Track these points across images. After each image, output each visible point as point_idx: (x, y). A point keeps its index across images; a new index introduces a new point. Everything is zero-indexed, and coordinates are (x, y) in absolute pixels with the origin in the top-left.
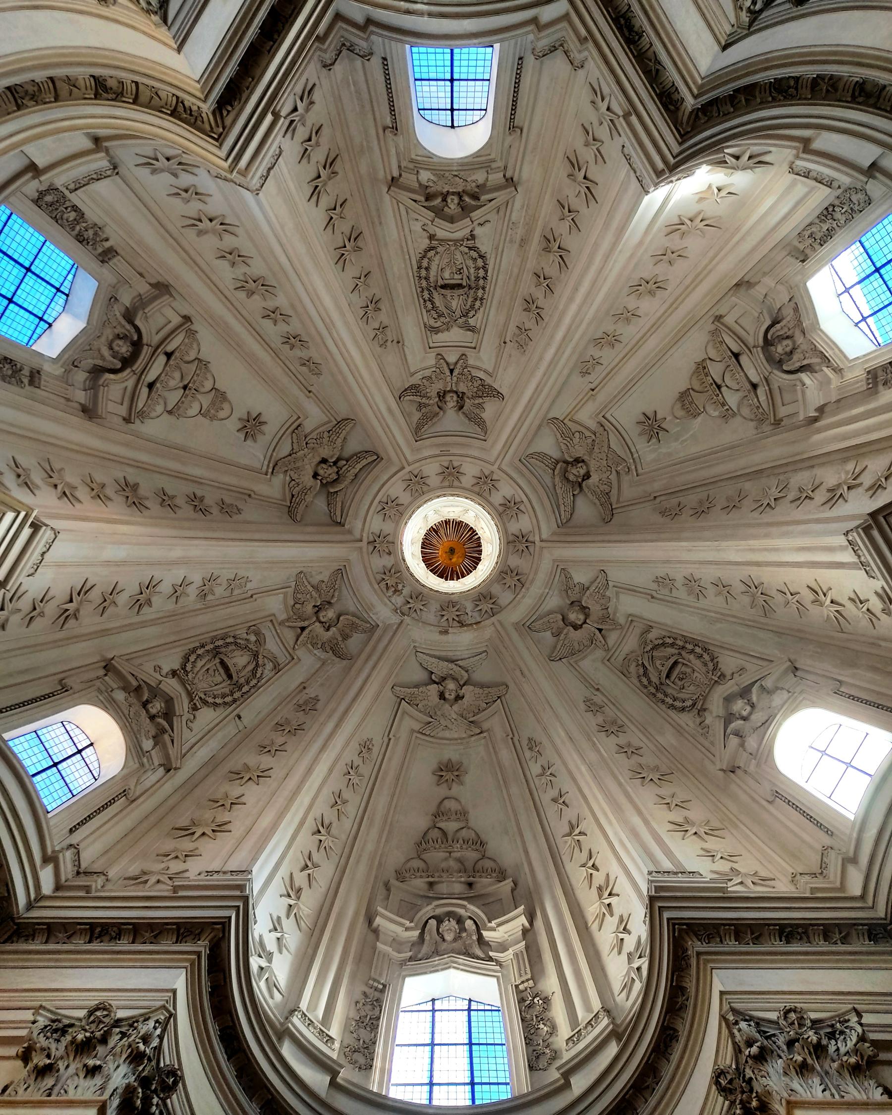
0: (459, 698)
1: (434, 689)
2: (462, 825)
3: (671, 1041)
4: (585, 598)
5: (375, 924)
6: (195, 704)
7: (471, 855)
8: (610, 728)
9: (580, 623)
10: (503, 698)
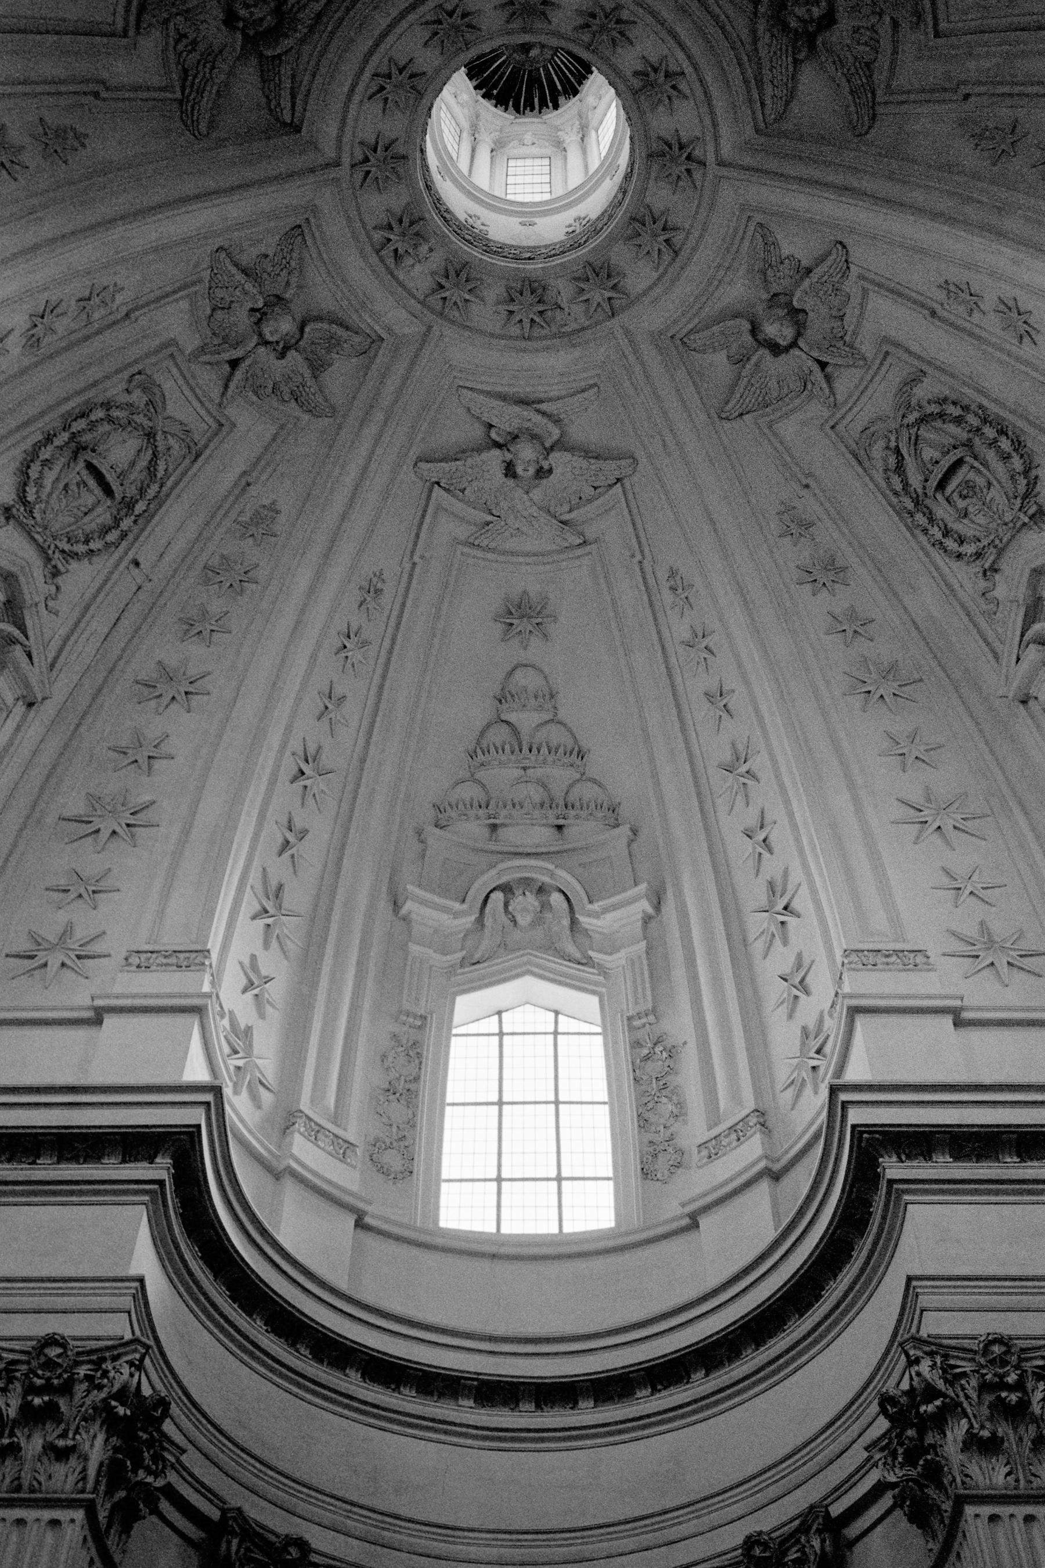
0: (542, 473)
1: (495, 458)
2: (547, 716)
4: (798, 294)
5: (403, 911)
6: (55, 567)
7: (560, 776)
8: (825, 573)
9: (783, 343)
10: (625, 481)
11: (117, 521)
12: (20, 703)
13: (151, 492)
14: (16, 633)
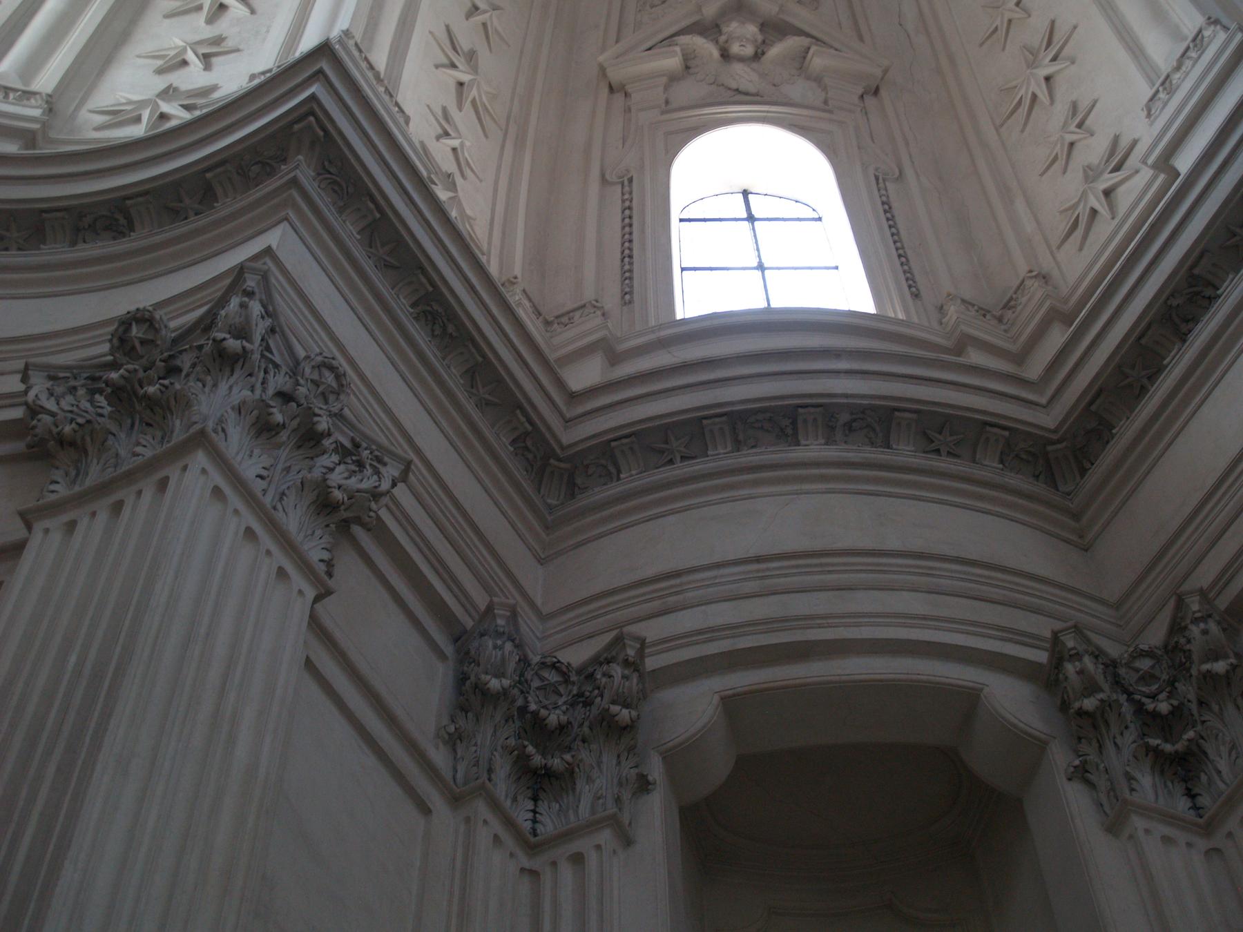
3: (107, 229)
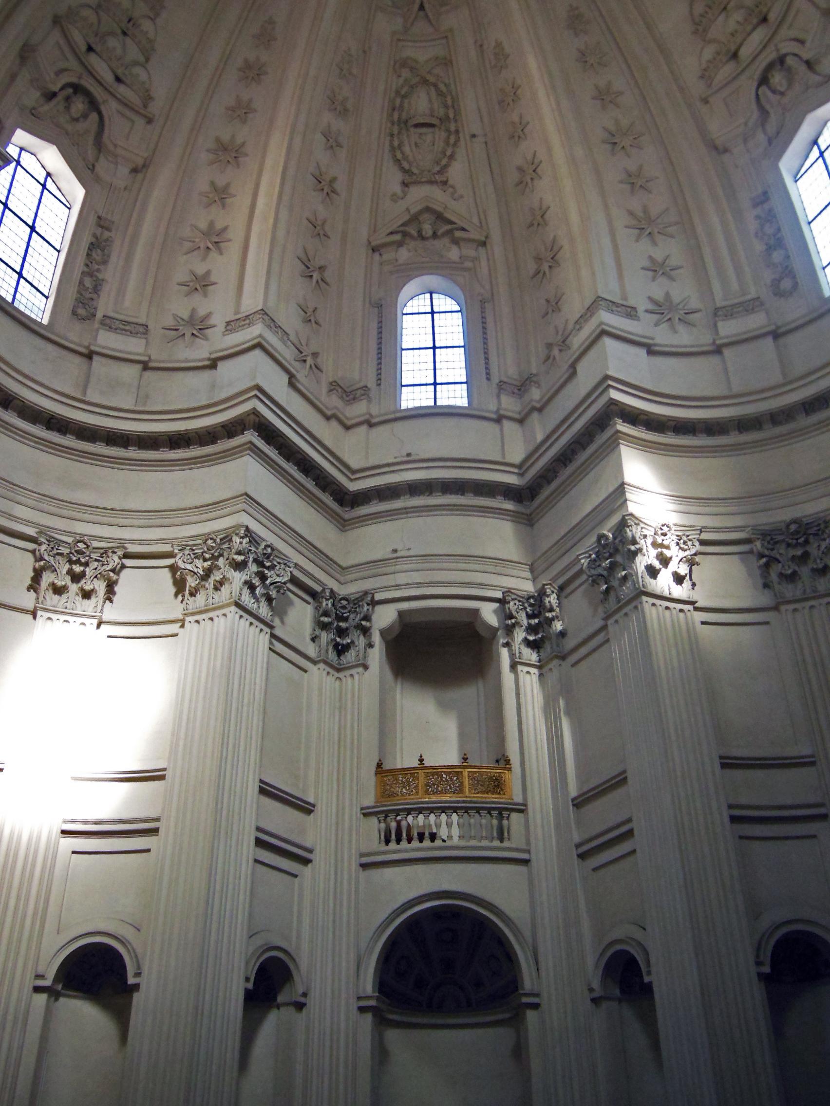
11: (448, 131)
12: (480, 248)
13: (449, 102)
14: (449, 227)
